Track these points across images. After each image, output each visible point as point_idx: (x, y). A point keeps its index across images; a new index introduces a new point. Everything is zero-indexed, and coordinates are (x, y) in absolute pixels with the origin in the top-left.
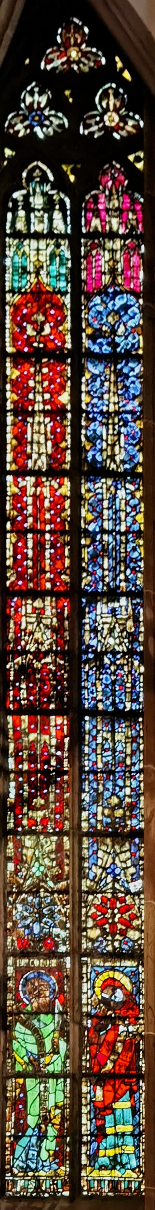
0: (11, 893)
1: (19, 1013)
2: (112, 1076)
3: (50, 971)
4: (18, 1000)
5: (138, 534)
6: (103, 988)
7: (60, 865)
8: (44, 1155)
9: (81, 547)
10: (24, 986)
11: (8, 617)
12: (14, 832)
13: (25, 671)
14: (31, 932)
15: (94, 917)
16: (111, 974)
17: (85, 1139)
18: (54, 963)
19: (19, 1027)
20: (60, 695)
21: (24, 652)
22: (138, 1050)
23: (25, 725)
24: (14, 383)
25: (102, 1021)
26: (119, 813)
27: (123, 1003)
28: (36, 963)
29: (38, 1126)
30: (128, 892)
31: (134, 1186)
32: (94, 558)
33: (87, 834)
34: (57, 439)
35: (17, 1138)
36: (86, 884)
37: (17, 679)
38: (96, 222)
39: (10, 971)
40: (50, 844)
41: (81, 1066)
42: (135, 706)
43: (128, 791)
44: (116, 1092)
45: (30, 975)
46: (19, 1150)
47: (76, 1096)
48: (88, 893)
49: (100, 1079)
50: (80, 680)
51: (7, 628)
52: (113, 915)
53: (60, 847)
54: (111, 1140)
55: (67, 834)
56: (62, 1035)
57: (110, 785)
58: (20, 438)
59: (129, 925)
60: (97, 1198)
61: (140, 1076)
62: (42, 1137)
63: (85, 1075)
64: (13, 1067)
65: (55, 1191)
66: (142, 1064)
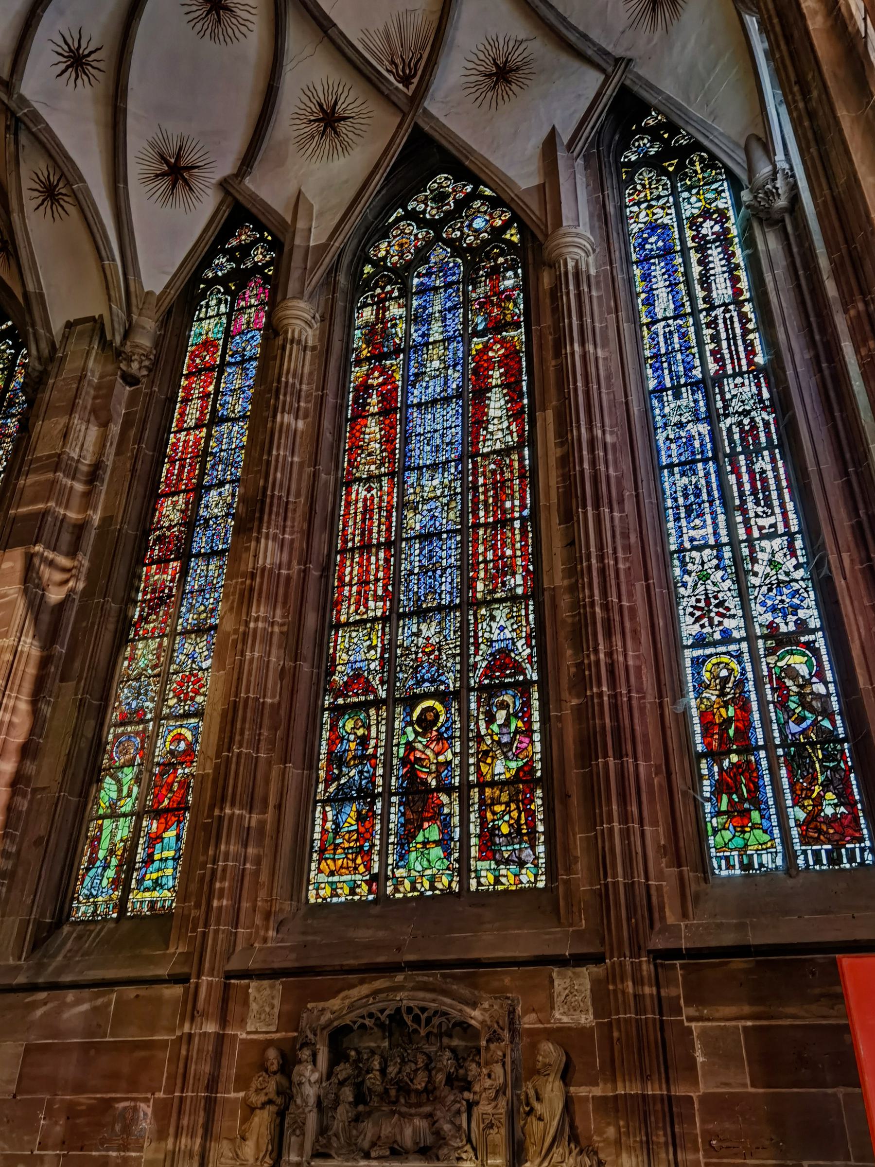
0: (122, 682)
1: (111, 768)
2: (167, 810)
3: (137, 733)
4: (111, 758)
5: (242, 447)
6: (171, 742)
7: (158, 658)
8: (105, 882)
9: (206, 462)
11: (155, 510)
12: (133, 640)
13: (160, 539)
14: (130, 707)
15: (174, 691)
16: (179, 730)
17: (137, 866)
18: (141, 727)
19: (108, 780)
20: (179, 548)
21: (162, 527)
22: (189, 787)
23: (153, 571)
24: (185, 388)
25: (168, 767)
26: (203, 616)
27: (184, 751)
28: (129, 729)
29: (105, 858)
30: (201, 669)
31: (167, 904)
34: (203, 408)
35: (88, 869)
36: (173, 667)
37: (154, 544)
38: (243, 303)
40: (153, 644)
41: (145, 805)
42: (225, 546)
43: (211, 600)
44: (167, 823)
45: (123, 739)
46: (87, 879)
47: (137, 831)
48: (173, 674)
49: (157, 813)
50: (193, 537)
51: (153, 516)
52: (188, 687)
53: (160, 645)
54: (156, 865)
55: (166, 636)
56: (136, 782)
57: (200, 599)
58: (182, 414)
59: (197, 692)
60: (139, 918)
61: (187, 809)
62: (106, 867)
63: (147, 812)
64: (97, 811)
65: (107, 914)
66: (190, 798)
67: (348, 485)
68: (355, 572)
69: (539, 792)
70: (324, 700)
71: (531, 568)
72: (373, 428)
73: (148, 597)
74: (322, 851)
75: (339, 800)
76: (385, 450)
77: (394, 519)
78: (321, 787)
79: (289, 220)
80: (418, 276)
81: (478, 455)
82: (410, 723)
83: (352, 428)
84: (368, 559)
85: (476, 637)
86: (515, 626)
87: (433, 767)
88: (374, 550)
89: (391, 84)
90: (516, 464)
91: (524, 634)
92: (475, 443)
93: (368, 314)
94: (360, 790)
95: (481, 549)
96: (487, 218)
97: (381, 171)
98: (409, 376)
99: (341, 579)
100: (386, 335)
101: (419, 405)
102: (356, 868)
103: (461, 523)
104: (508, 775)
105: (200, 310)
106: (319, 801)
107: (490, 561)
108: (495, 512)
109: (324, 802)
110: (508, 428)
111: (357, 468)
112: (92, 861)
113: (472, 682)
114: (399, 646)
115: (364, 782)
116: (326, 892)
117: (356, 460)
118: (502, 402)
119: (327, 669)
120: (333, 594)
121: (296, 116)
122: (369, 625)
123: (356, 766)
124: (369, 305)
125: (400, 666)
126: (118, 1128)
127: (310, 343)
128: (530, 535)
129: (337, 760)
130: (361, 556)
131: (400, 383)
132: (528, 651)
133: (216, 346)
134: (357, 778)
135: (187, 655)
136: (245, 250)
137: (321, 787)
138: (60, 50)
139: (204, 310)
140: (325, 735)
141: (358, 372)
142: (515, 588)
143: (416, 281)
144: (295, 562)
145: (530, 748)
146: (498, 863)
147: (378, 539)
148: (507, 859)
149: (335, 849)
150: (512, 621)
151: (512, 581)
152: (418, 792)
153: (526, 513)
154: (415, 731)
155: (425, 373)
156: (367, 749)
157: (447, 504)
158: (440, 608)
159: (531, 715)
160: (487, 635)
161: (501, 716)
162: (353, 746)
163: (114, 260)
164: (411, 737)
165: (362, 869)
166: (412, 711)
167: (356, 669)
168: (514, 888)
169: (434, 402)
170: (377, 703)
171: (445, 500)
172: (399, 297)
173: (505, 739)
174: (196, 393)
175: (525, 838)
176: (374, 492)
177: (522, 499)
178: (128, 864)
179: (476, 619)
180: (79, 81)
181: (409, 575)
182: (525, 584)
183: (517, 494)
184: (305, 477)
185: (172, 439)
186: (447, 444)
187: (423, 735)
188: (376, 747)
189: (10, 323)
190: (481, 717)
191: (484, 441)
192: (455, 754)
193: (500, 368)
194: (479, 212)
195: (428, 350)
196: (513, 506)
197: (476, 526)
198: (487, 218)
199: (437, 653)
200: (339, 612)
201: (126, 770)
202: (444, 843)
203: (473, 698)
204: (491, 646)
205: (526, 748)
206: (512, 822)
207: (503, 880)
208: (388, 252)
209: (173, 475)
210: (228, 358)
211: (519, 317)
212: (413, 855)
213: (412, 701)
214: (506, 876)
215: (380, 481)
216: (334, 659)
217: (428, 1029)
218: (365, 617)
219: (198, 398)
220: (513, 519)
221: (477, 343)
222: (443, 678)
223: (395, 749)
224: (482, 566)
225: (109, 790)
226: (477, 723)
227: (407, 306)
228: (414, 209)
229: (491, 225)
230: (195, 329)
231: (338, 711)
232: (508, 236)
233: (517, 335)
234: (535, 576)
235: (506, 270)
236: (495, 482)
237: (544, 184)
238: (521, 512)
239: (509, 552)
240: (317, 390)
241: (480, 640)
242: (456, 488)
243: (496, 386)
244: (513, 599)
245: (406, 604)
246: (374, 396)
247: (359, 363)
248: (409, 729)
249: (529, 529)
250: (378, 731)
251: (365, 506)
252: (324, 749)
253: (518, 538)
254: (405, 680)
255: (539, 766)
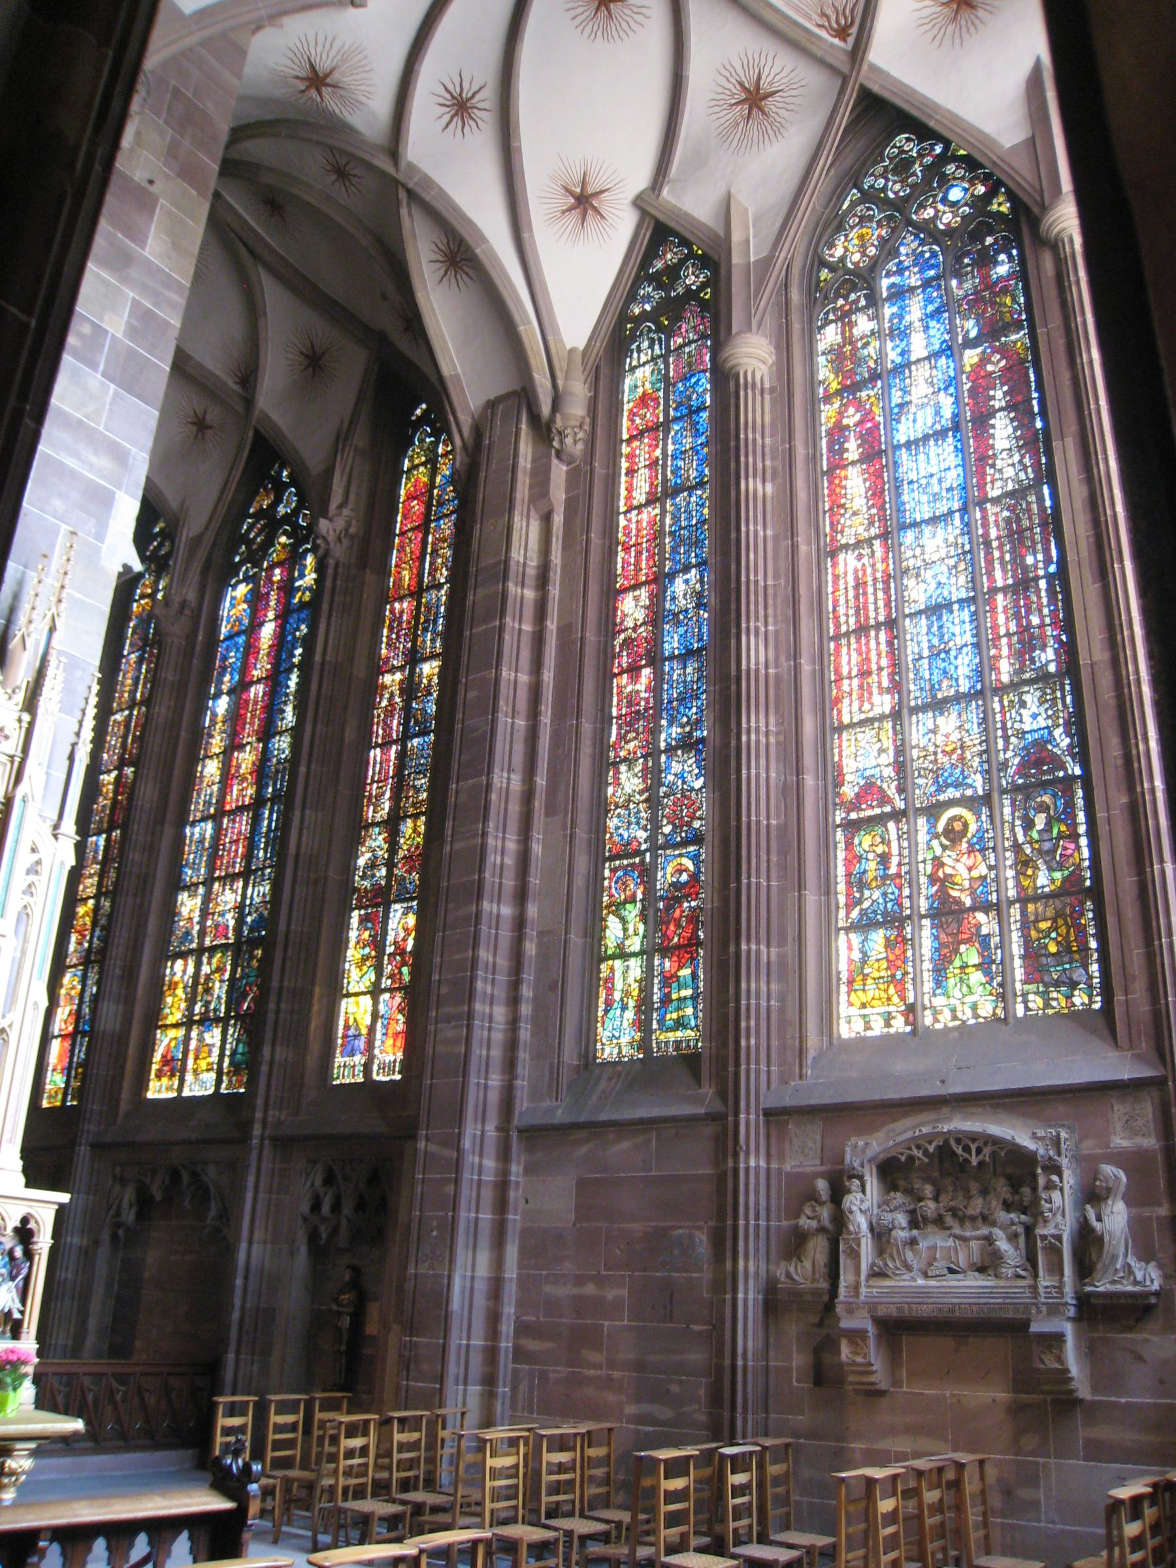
2: (678, 947)
4: (611, 896)
8: (625, 1024)
10: (616, 882)
11: (616, 609)
13: (628, 642)
18: (637, 860)
19: (611, 918)
21: (626, 629)
22: (698, 921)
25: (673, 901)
26: (687, 729)
27: (686, 883)
29: (622, 1000)
30: (693, 789)
32: (674, 550)
33: (665, 751)
35: (606, 1011)
36: (663, 790)
39: (607, 873)
45: (620, 873)
47: (649, 970)
51: (615, 616)
52: (682, 811)
54: (675, 1004)
58: (629, 490)
59: (693, 817)
60: (665, 1059)
62: (624, 1008)
66: (700, 933)
67: (833, 554)
68: (853, 662)
69: (1089, 904)
70: (834, 815)
71: (1064, 638)
72: (855, 483)
73: (624, 712)
74: (850, 982)
75: (864, 925)
76: (873, 506)
77: (893, 591)
78: (842, 913)
79: (722, 233)
80: (888, 275)
81: (987, 500)
82: (937, 836)
83: (831, 482)
84: (867, 644)
85: (1004, 728)
86: (1050, 712)
87: (966, 884)
88: (873, 633)
89: (825, 41)
90: (1034, 507)
91: (1061, 721)
92: (982, 486)
93: (830, 335)
94: (885, 914)
95: (1001, 619)
96: (966, 185)
97: (825, 153)
98: (891, 409)
99: (838, 671)
100: (858, 361)
101: (908, 444)
102: (889, 999)
103: (974, 589)
104: (1053, 887)
105: (631, 357)
106: (841, 929)
107: (1014, 634)
108: (1014, 571)
109: (847, 930)
110: (1020, 462)
111: (842, 532)
112: (609, 1004)
113: (1004, 782)
114: (914, 747)
115: (889, 905)
116: (858, 1025)
117: (838, 522)
118: (1010, 430)
119: (834, 780)
120: (831, 690)
121: (715, 103)
122: (876, 725)
123: (878, 887)
124: (832, 322)
125: (919, 770)
126: (676, 1252)
127: (767, 385)
128: (1060, 597)
129: (858, 883)
130: (858, 641)
131: (881, 419)
132: (1068, 740)
133: (656, 400)
134: (881, 901)
135: (676, 775)
136: (673, 272)
137: (842, 913)
138: (442, 101)
139: (635, 355)
140: (841, 855)
141: (828, 413)
142: (1046, 664)
143: (885, 283)
144: (783, 659)
145: (1076, 855)
146: (1046, 985)
147: (876, 618)
148: (1057, 980)
149: (864, 980)
150: (1047, 706)
151: (1043, 656)
152: (953, 912)
153: (1052, 569)
154: (942, 845)
155: (911, 402)
156: (888, 868)
157: (955, 567)
158: (958, 698)
159: (1076, 816)
160: (1017, 725)
161: (1040, 821)
162: (872, 865)
163: (529, 323)
164: (938, 851)
165: (896, 999)
166: (937, 819)
167: (867, 778)
168: (1066, 1011)
169: (926, 438)
170: (897, 815)
171: (952, 562)
172: (867, 307)
173: (1047, 846)
174: (642, 461)
175: (1077, 956)
176: (865, 560)
177: (1047, 551)
178: (644, 1005)
179: (1002, 707)
180: (467, 129)
181: (917, 660)
182: (1058, 661)
183: (1039, 546)
184: (782, 553)
185: (622, 522)
186: (948, 490)
187: (952, 848)
188: (900, 865)
189: (424, 406)
190: (1018, 822)
191: (992, 482)
192: (990, 868)
193: (1002, 385)
194: (955, 179)
195: (910, 372)
196: (1037, 562)
197: (994, 590)
198: (966, 185)
199: (959, 752)
200: (840, 712)
201: (628, 906)
202: (985, 966)
203: (1007, 802)
204: (1023, 738)
205: (1071, 855)
206: (1059, 939)
207: (1054, 1003)
208: (846, 249)
209: (629, 564)
210: (672, 413)
211: (1020, 314)
212: (951, 982)
213: (933, 811)
214: (1057, 999)
215: (871, 546)
216: (840, 768)
217: (981, 1157)
218: (871, 715)
219: (645, 467)
220: (1037, 578)
221: (971, 357)
222: (969, 781)
223: (921, 866)
224: (1004, 641)
225: (613, 930)
226: (1012, 830)
227: (877, 317)
228: (872, 187)
229: (973, 195)
230: (628, 382)
231: (853, 827)
232: (995, 207)
233: (1018, 338)
234: (1069, 652)
235: (998, 252)
236: (1010, 534)
237: (1033, 137)
238: (1046, 568)
239: (1035, 620)
240: (783, 443)
241: (1010, 732)
242: (963, 545)
243: (1001, 409)
244: (1043, 678)
245: (915, 694)
246: (852, 439)
247: (828, 399)
248: (935, 843)
249: (1058, 589)
250: (900, 847)
251: (856, 578)
252: (841, 871)
253: (1045, 601)
254: (923, 787)
255: (1088, 875)
